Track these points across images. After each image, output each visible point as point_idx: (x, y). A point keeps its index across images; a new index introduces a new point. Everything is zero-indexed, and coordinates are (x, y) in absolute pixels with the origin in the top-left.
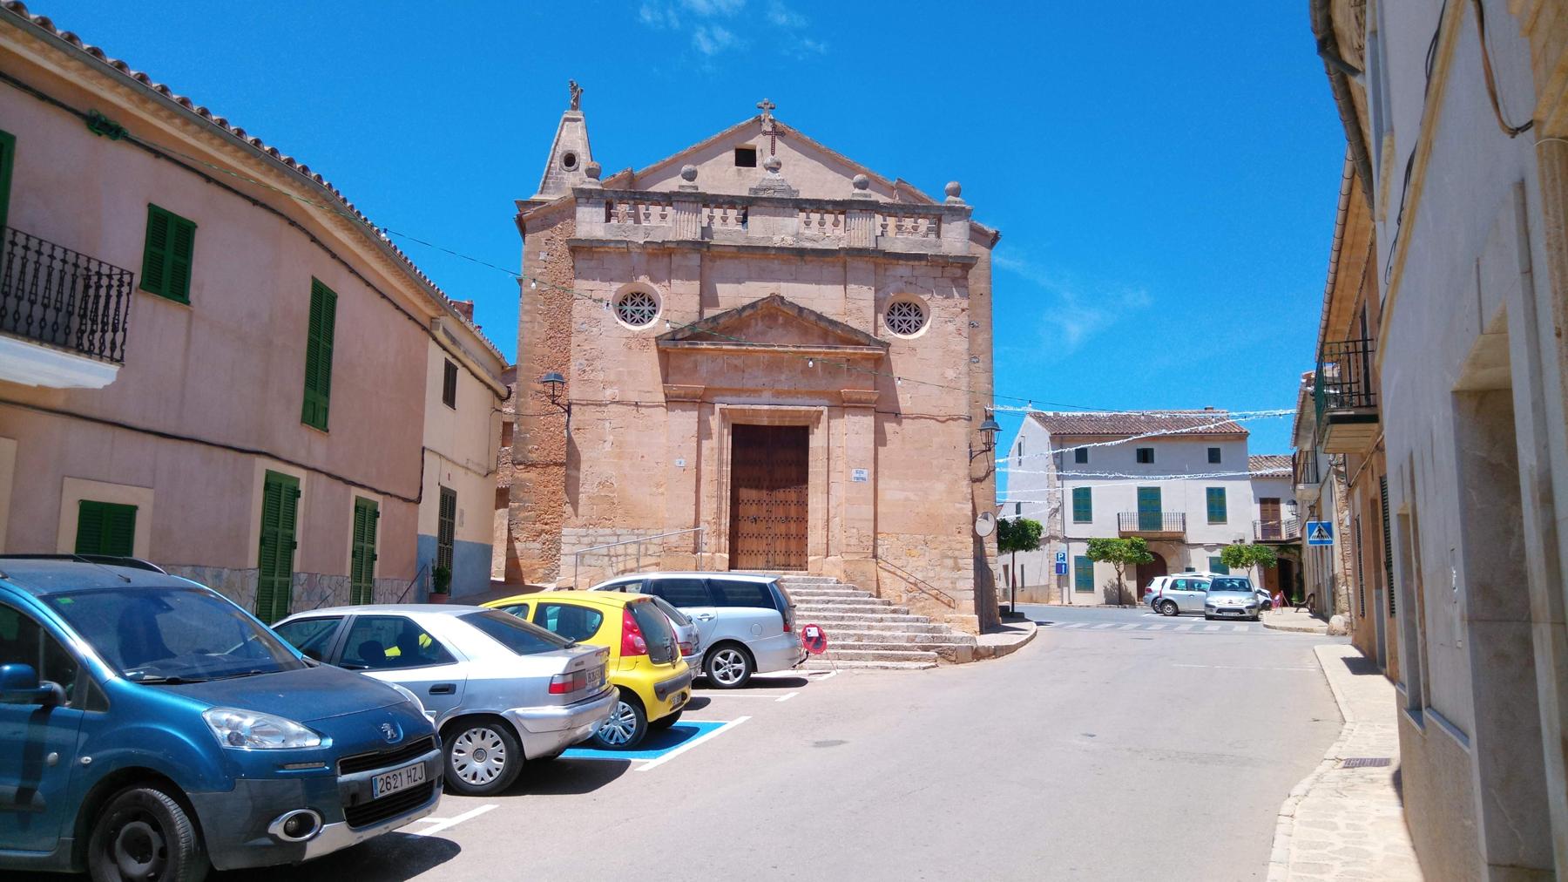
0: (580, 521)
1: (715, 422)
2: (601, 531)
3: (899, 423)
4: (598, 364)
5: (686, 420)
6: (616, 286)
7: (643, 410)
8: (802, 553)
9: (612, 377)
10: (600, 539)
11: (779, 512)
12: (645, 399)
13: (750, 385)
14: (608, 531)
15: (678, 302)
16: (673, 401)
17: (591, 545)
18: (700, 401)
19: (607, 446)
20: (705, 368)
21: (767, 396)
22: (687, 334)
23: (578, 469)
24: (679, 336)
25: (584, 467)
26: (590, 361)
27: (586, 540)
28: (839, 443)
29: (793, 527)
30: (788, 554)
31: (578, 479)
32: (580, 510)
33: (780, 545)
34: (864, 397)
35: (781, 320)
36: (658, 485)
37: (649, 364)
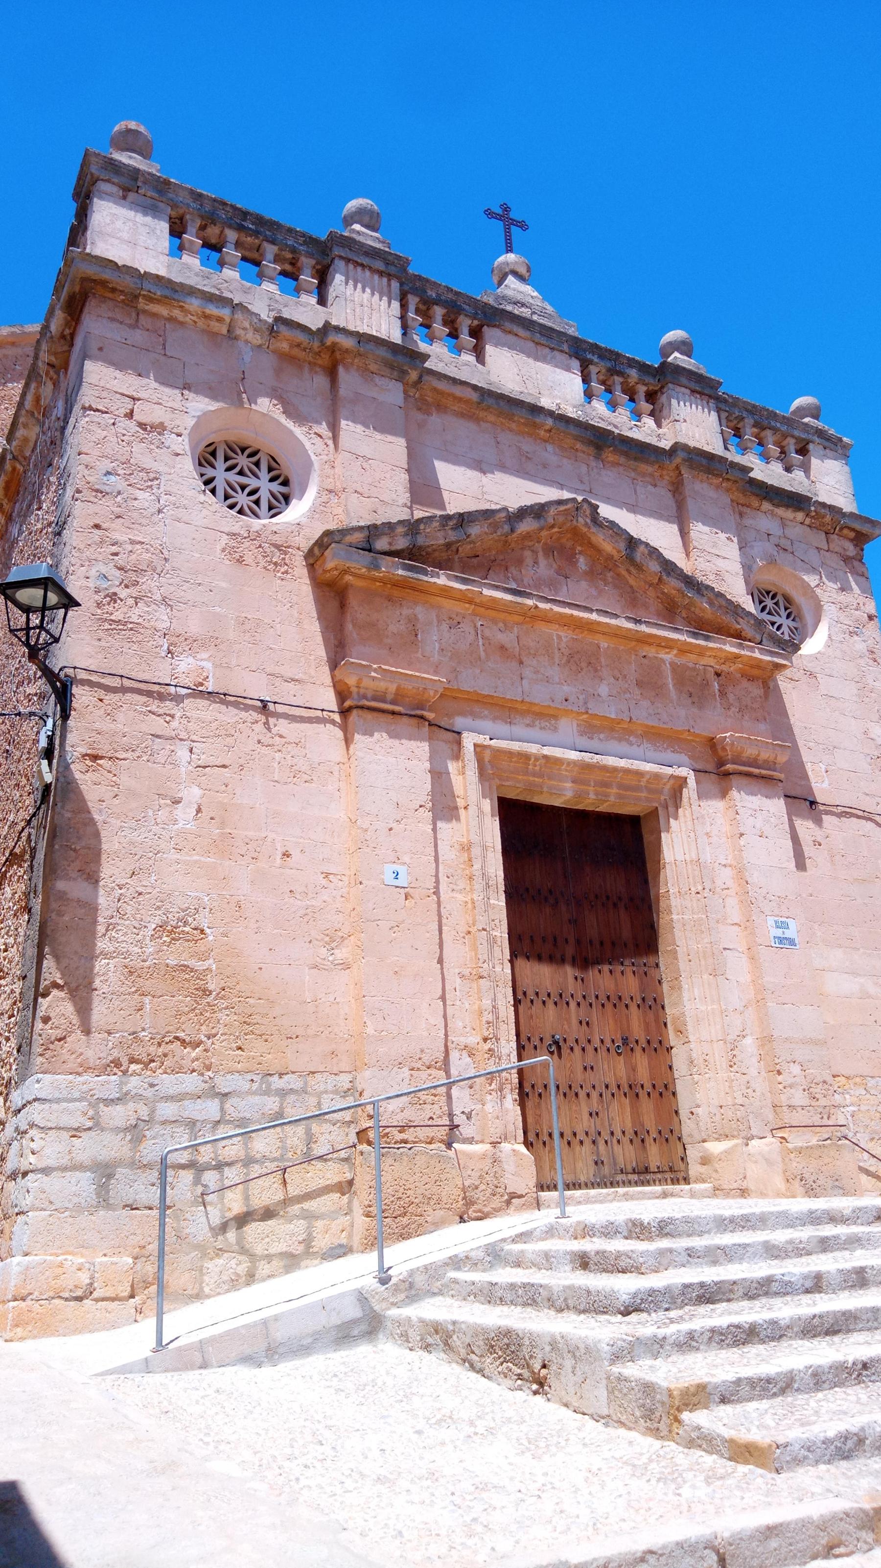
0: (96, 1049)
1: (465, 781)
2: (168, 1083)
3: (819, 822)
4: (148, 583)
5: (396, 762)
6: (200, 405)
7: (282, 726)
8: (670, 1135)
9: (194, 627)
10: (167, 1110)
11: (605, 1028)
12: (287, 693)
13: (539, 695)
14: (191, 1082)
15: (354, 474)
16: (354, 709)
17: (135, 1132)
18: (422, 715)
19: (184, 815)
20: (435, 638)
21: (567, 727)
22: (401, 543)
23: (93, 878)
24: (382, 544)
25: (111, 871)
26: (132, 575)
27: (118, 1115)
28: (714, 851)
29: (642, 1062)
30: (639, 1138)
31: (92, 909)
32: (100, 1012)
33: (620, 1116)
34: (765, 755)
35: (582, 563)
36: (333, 940)
37: (291, 616)
